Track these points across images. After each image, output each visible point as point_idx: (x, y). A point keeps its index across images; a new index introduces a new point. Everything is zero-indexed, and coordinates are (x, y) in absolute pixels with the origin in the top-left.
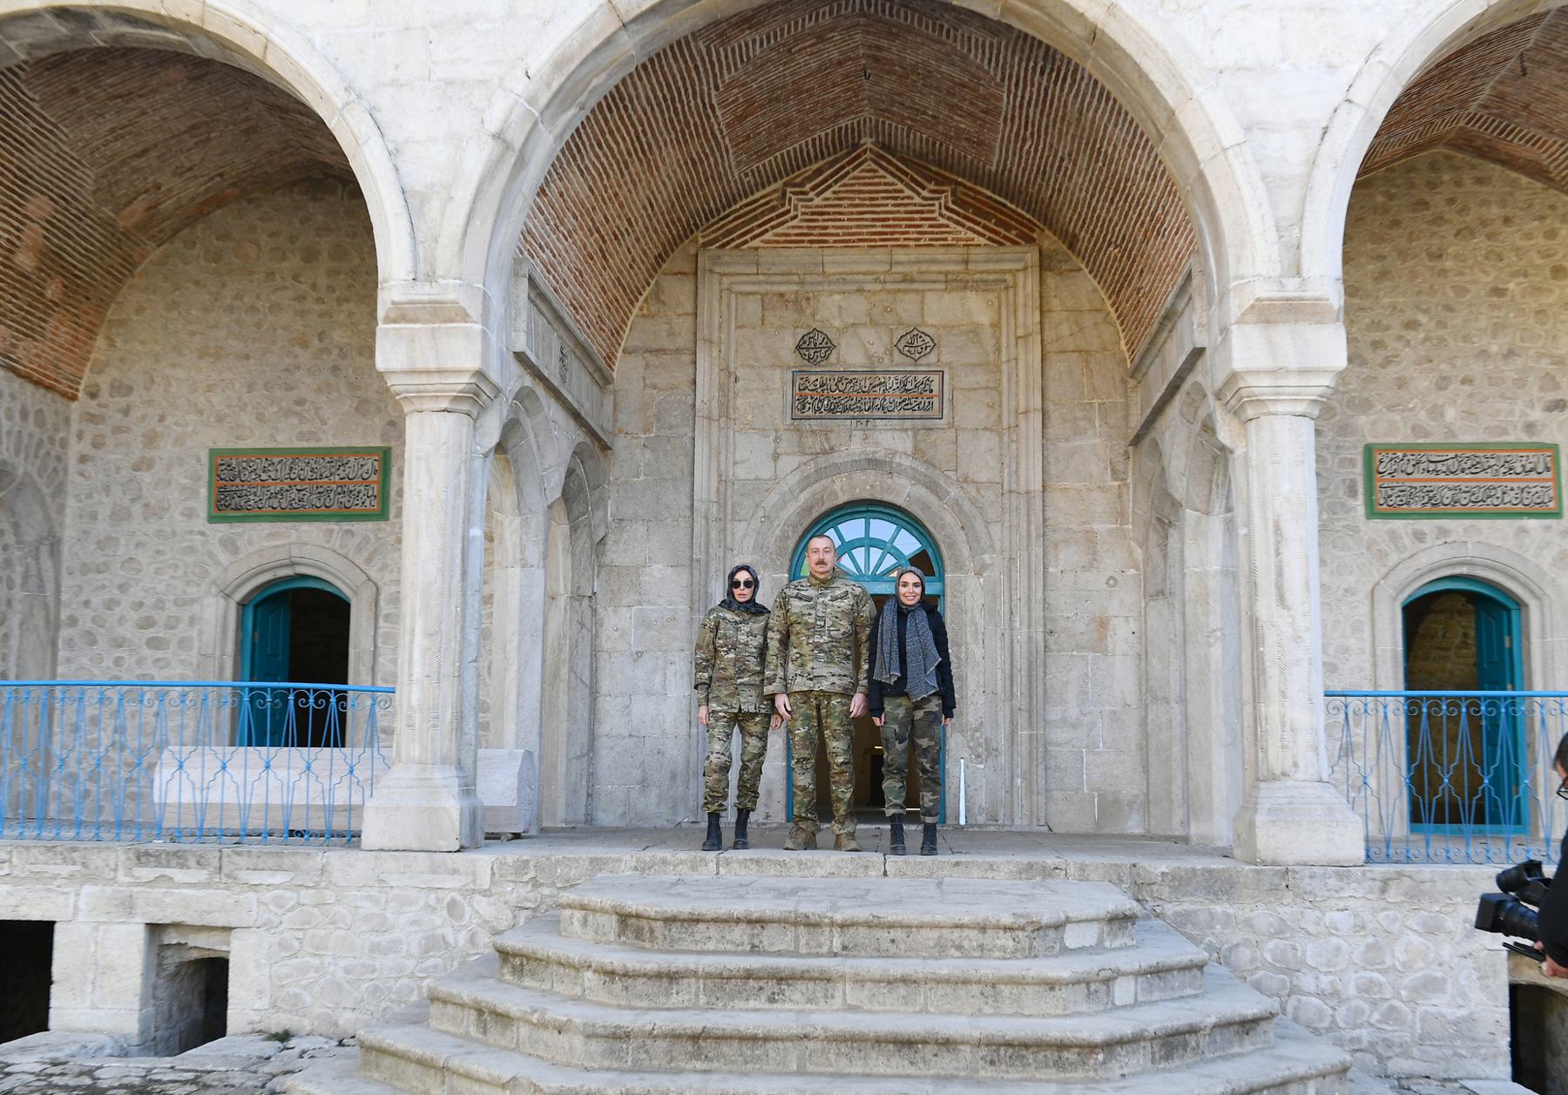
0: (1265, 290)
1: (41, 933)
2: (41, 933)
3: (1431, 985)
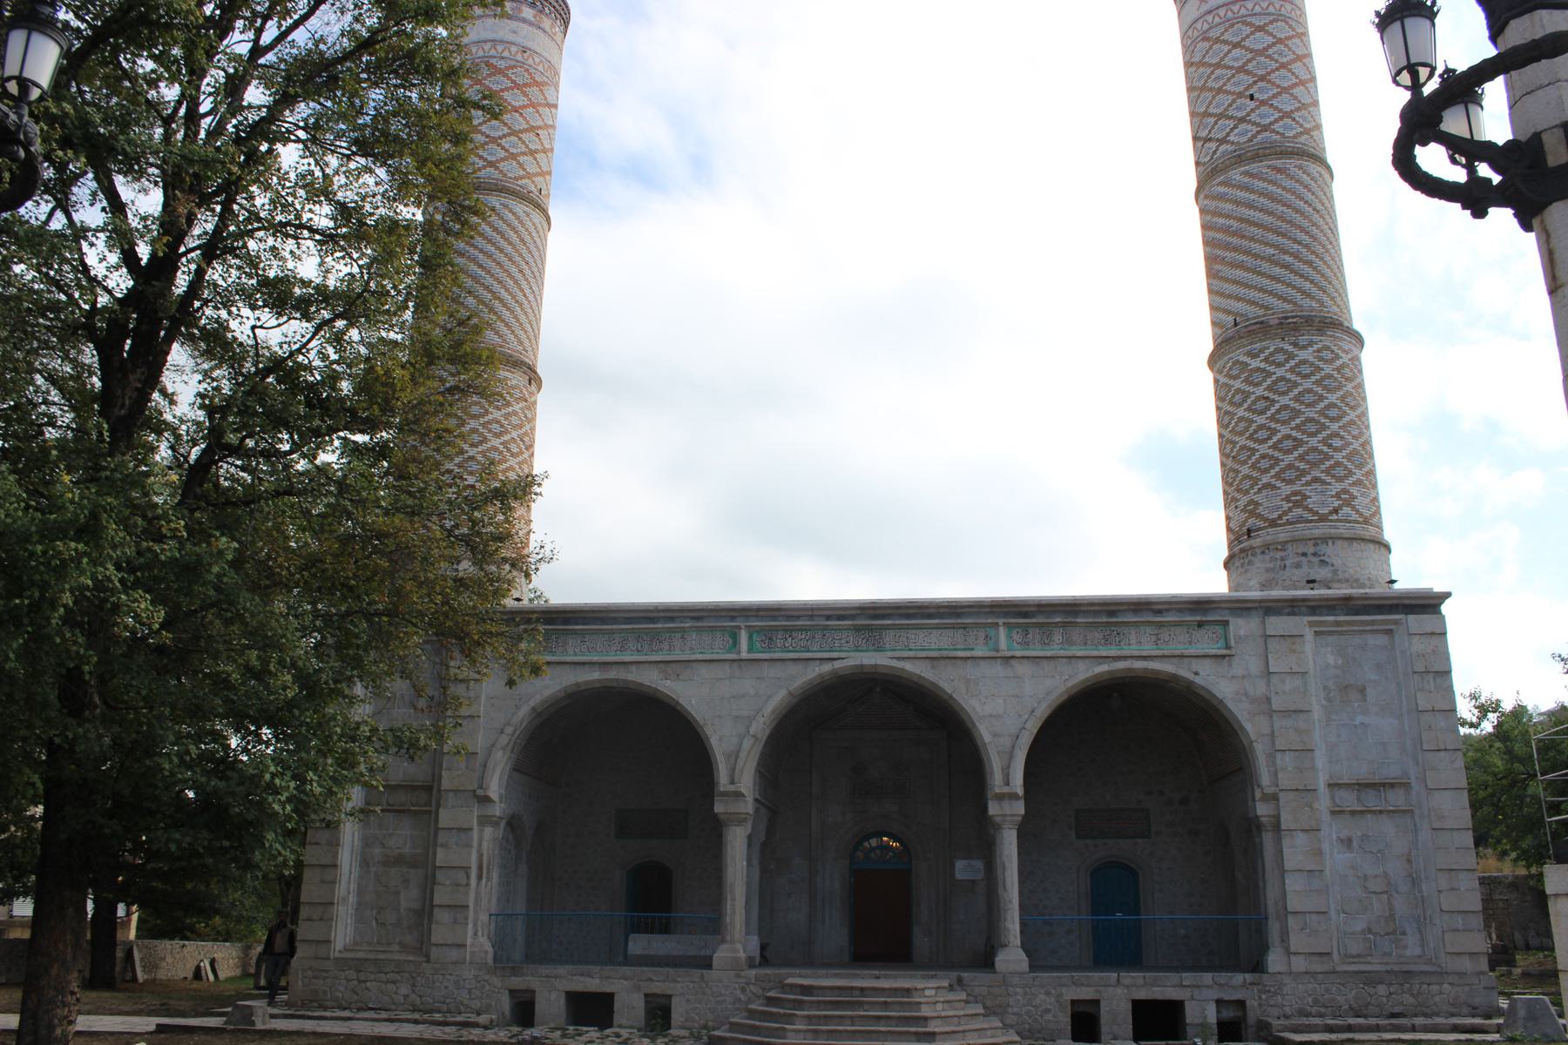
0: (997, 790)
1: (611, 996)
2: (611, 996)
3: (1048, 1011)
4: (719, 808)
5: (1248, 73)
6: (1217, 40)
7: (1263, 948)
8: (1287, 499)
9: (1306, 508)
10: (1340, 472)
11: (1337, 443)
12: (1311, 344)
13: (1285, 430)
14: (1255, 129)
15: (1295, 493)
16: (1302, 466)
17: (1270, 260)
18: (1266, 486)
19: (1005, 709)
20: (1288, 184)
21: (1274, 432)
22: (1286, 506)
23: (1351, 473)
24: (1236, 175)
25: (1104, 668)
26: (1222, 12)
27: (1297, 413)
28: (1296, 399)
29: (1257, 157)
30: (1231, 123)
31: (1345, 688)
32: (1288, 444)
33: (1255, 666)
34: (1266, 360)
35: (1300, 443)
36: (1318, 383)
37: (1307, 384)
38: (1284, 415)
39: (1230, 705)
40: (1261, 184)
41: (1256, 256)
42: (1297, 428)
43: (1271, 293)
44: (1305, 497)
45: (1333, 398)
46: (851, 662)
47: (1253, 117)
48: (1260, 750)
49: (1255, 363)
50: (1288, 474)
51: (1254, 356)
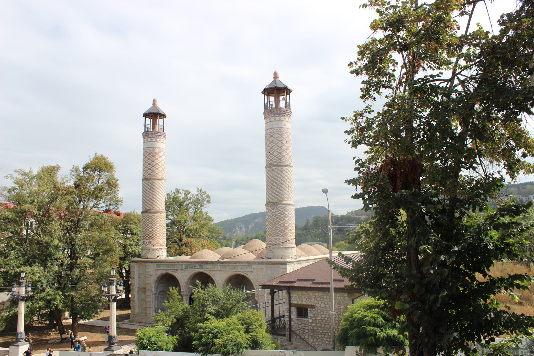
10: (278, 234)
11: (277, 229)
20: (274, 173)
45: (277, 219)
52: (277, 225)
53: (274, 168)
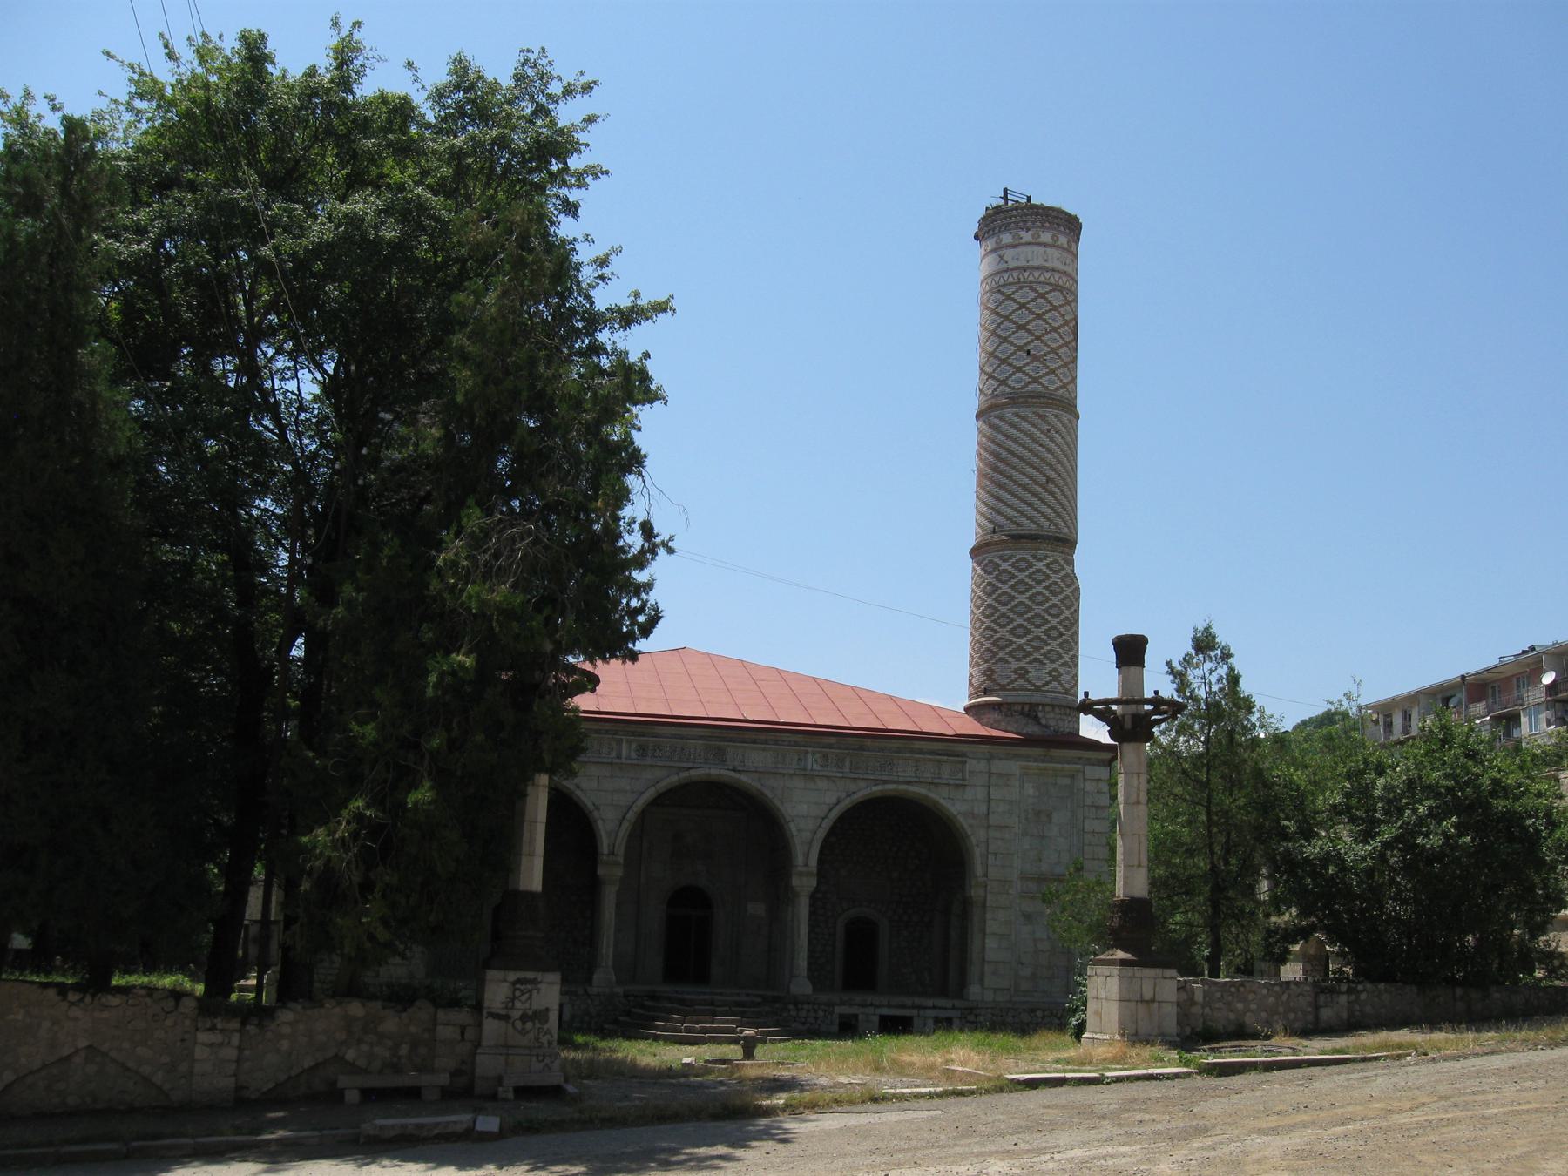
4: (601, 871)
5: (1029, 331)
6: (1009, 297)
7: (963, 984)
8: (1015, 672)
9: (1028, 681)
12: (1046, 557)
13: (1019, 620)
14: (1028, 380)
15: (1021, 668)
16: (1028, 649)
17: (1024, 486)
18: (1002, 660)
19: (808, 808)
21: (1012, 620)
22: (1014, 676)
23: (1061, 657)
24: (1009, 414)
25: (879, 788)
26: (1015, 274)
27: (1030, 609)
28: (1030, 598)
29: (1026, 404)
30: (1011, 370)
31: (1038, 813)
32: (1020, 631)
33: (980, 793)
34: (1012, 565)
35: (1029, 632)
36: (1046, 588)
37: (1039, 588)
38: (1021, 609)
39: (961, 818)
40: (1025, 425)
41: (1015, 482)
42: (1028, 620)
43: (1022, 513)
44: (1027, 672)
45: (1055, 600)
46: (701, 771)
47: (1027, 369)
48: (978, 852)
49: (1004, 566)
50: (1019, 654)
51: (1005, 560)
52: (1054, 622)
53: (1049, 413)
